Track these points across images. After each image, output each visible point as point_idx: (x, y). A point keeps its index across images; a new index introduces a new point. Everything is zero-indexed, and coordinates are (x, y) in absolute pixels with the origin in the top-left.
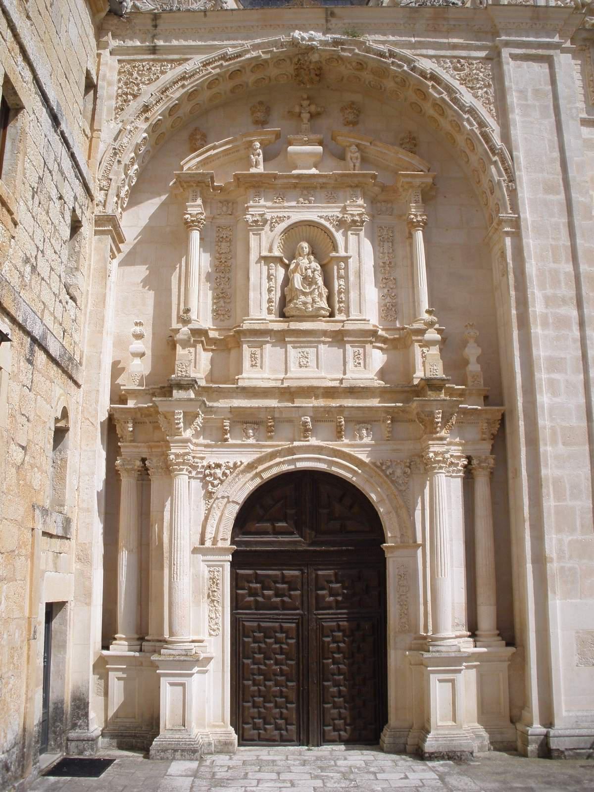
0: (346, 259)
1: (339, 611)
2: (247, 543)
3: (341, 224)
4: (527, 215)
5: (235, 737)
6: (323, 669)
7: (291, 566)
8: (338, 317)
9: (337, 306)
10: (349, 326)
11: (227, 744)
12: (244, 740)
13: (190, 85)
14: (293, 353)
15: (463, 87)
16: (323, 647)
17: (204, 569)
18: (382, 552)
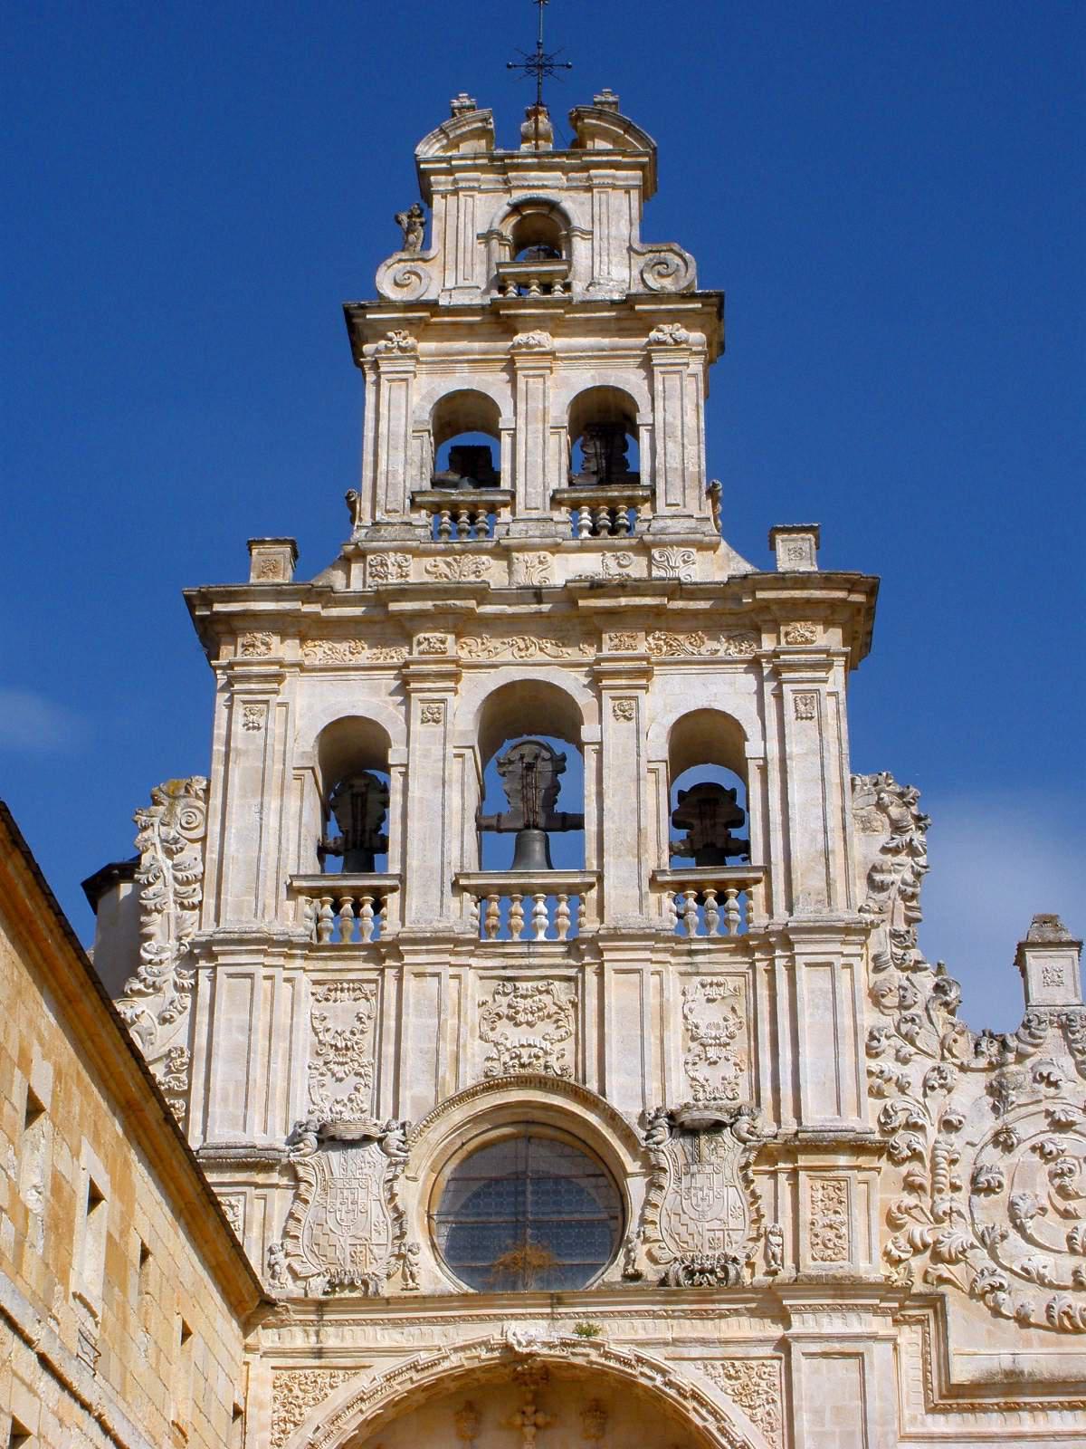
13: (370, 1409)
15: (737, 1407)
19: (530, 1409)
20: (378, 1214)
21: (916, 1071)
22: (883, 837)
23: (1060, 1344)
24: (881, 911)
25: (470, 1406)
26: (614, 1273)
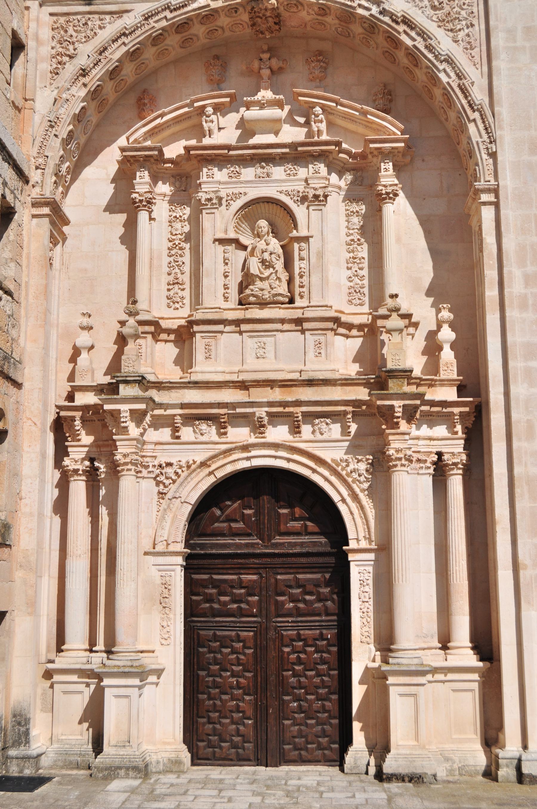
0: (306, 239)
1: (300, 619)
2: (202, 546)
4: (508, 182)
5: (186, 756)
6: (282, 682)
7: (248, 569)
8: (299, 303)
9: (297, 290)
10: (309, 314)
11: (178, 762)
12: (197, 759)
13: (131, 43)
14: (250, 343)
16: (282, 658)
17: (155, 574)
18: (345, 555)
19: (265, 56)
25: (217, 57)
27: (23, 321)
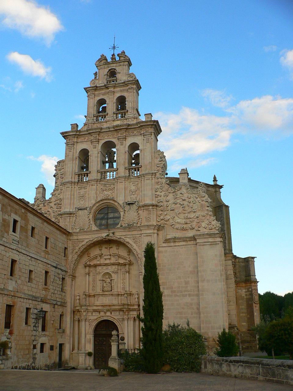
3: (113, 272)
5: (93, 367)
13: (84, 247)
15: (134, 244)
20: (87, 219)
21: (162, 194)
22: (159, 159)
23: (182, 232)
24: (158, 170)
26: (119, 226)
27: (67, 296)
